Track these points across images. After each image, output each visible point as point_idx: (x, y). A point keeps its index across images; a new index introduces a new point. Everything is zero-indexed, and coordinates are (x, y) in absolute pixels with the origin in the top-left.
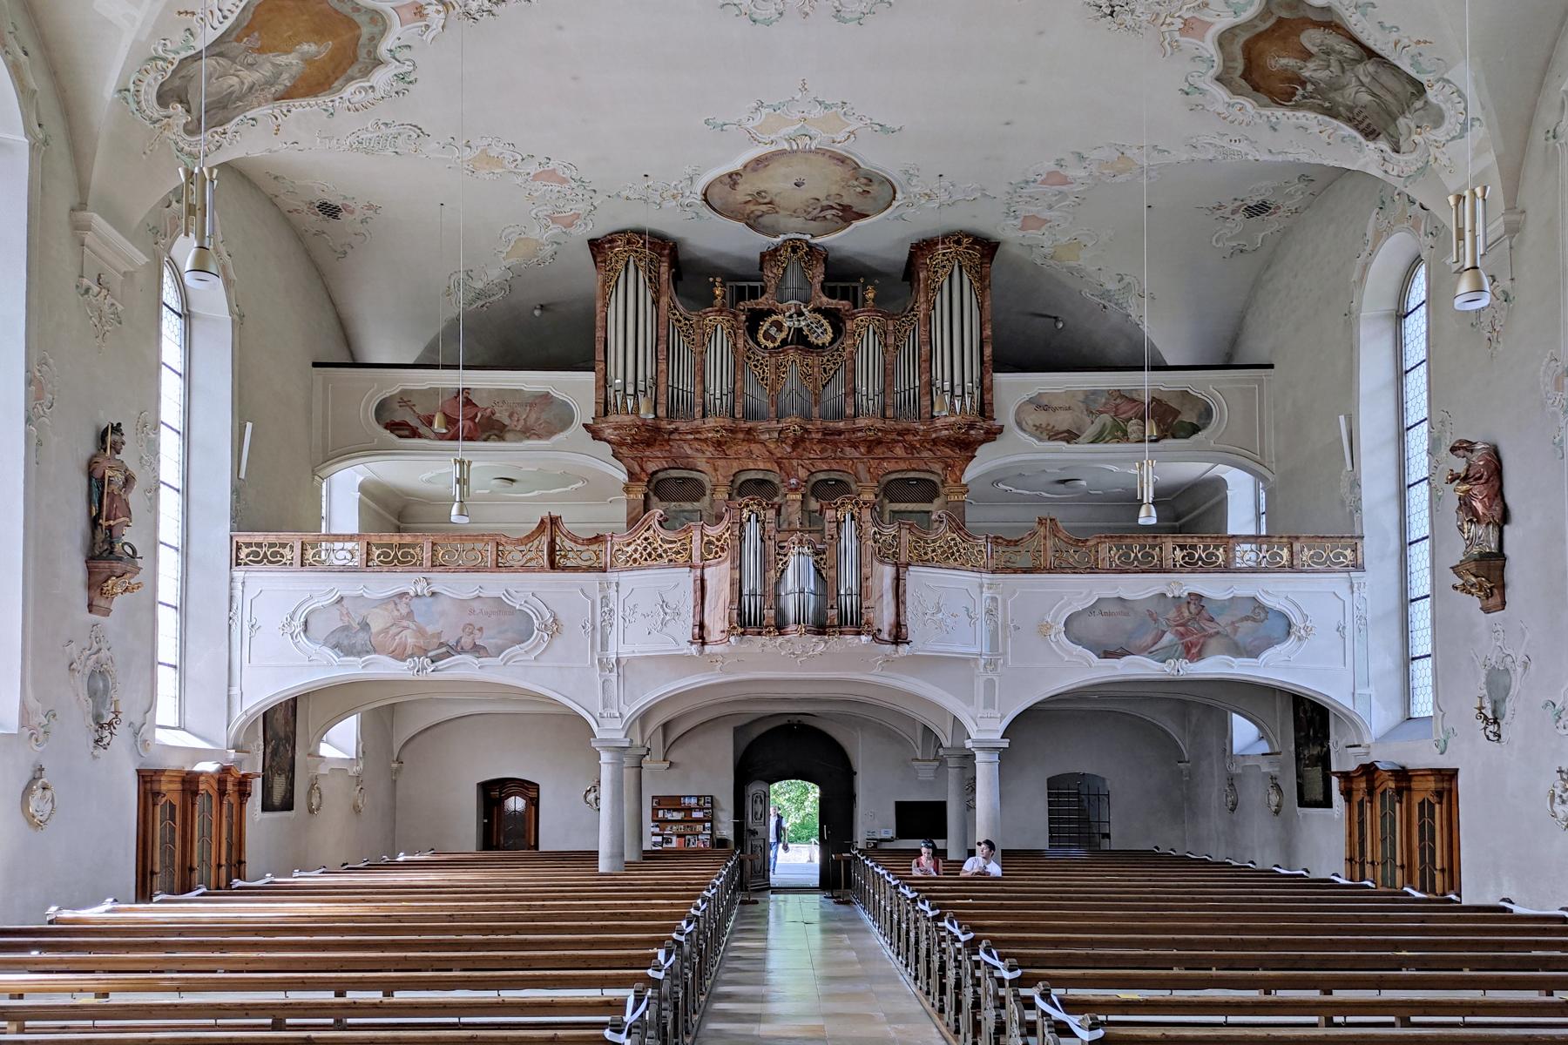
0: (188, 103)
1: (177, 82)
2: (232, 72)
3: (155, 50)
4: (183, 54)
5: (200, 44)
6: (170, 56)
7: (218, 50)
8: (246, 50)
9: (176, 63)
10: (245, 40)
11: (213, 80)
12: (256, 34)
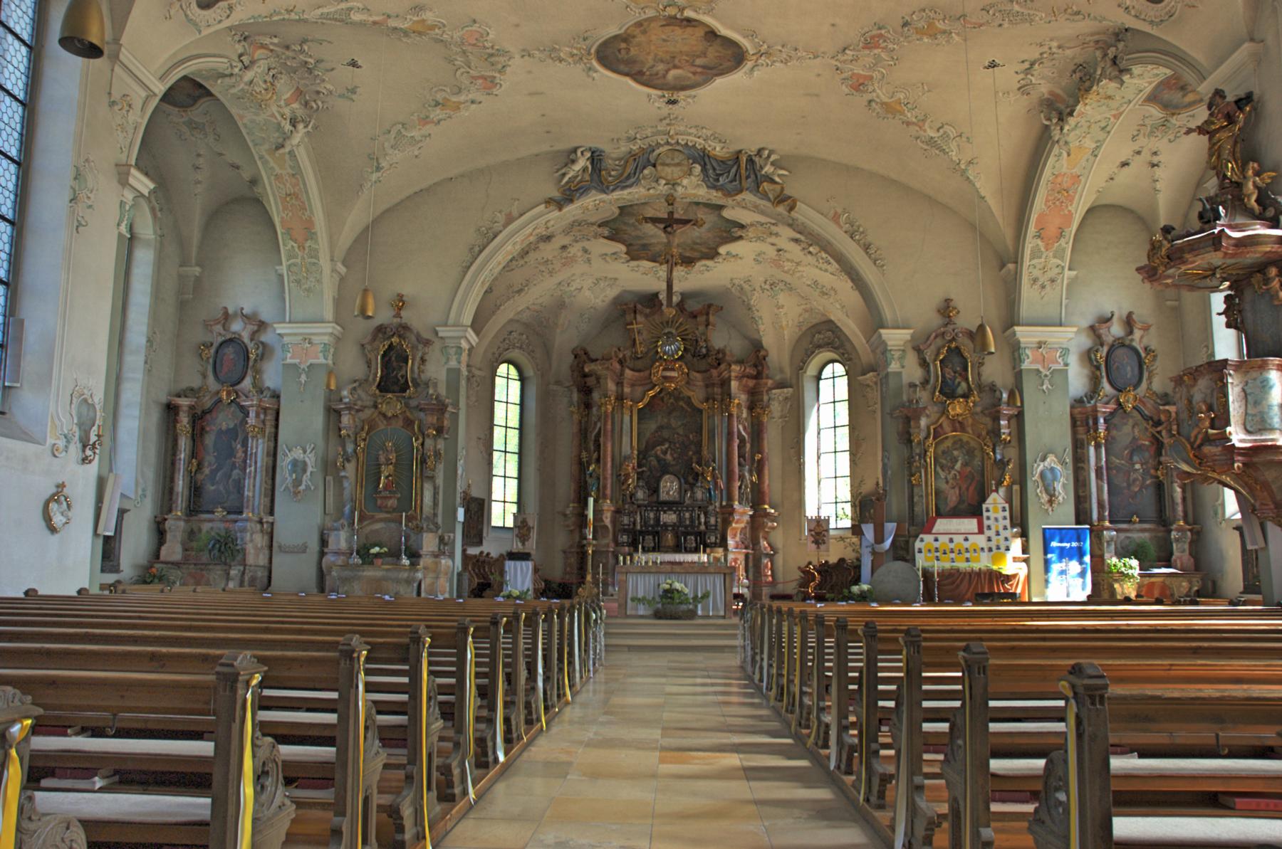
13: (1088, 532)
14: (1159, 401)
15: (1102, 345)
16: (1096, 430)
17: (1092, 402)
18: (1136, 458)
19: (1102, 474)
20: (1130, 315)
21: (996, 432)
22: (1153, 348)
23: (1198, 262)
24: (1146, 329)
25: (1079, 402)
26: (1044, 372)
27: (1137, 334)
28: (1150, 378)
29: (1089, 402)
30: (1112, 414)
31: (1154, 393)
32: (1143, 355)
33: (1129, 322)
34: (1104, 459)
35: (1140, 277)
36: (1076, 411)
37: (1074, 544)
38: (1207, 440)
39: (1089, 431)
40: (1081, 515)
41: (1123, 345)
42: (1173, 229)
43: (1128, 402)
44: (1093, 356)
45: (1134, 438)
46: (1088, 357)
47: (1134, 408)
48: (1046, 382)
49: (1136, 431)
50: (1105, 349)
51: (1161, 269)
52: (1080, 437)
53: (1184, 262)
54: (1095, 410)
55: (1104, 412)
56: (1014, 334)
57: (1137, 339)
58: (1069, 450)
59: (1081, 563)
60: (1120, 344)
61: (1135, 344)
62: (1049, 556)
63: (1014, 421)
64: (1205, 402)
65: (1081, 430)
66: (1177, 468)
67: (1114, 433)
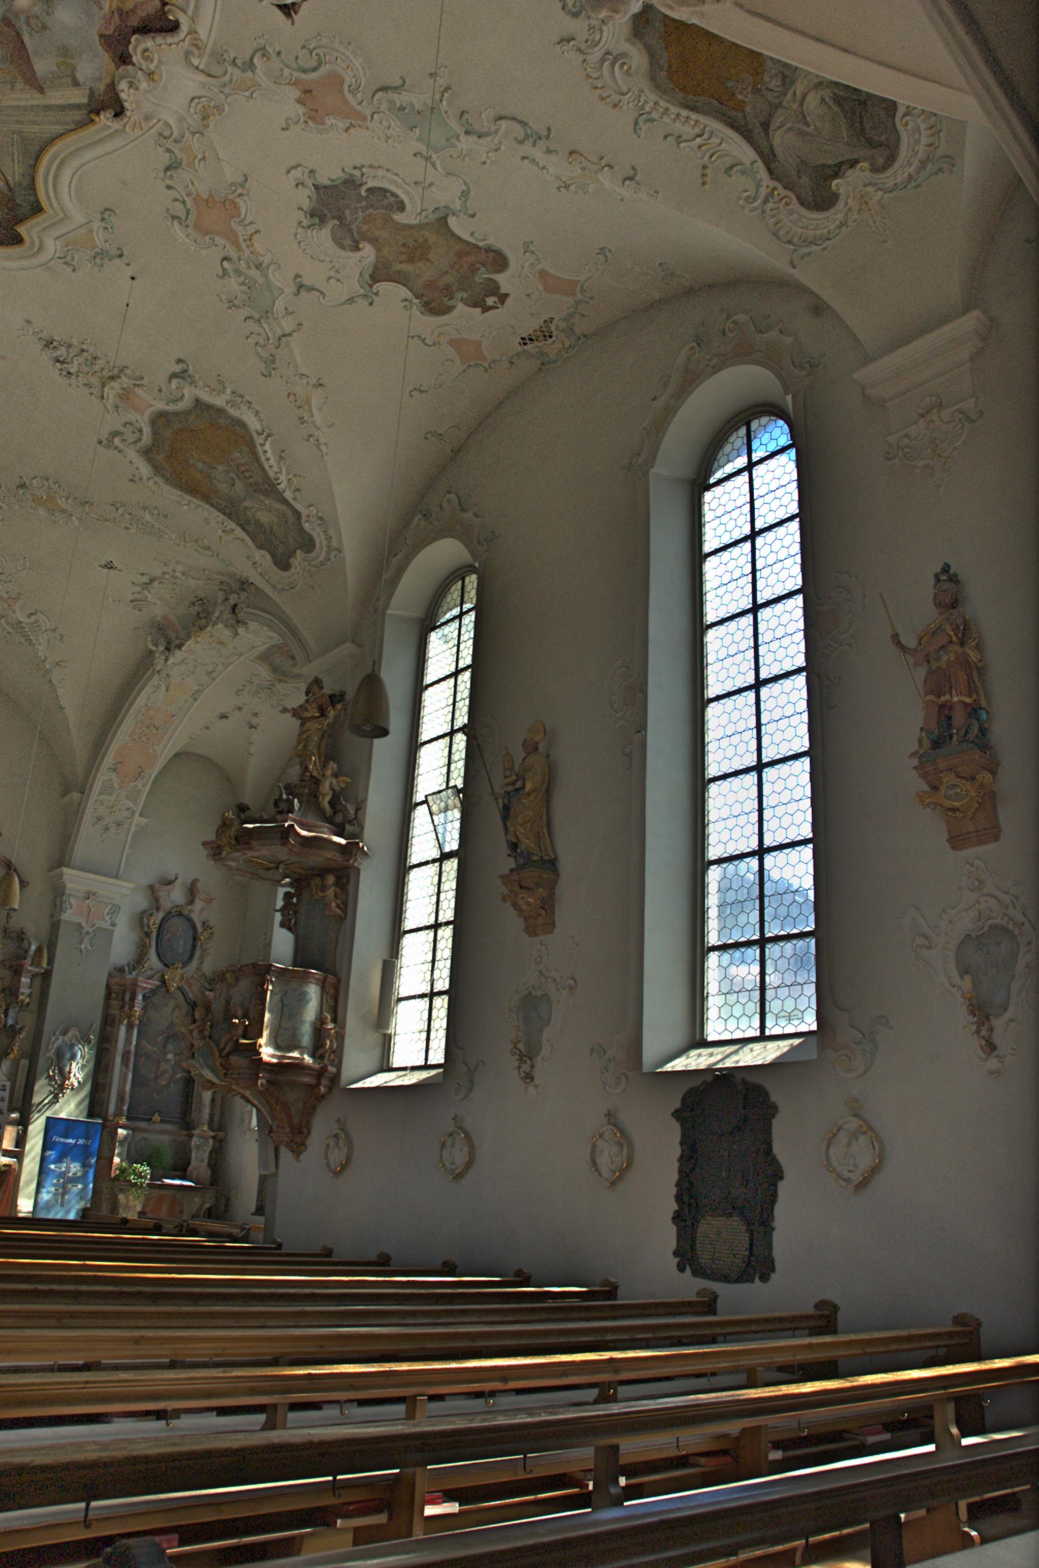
0: (841, 163)
1: (805, 180)
2: (795, 106)
3: (753, 210)
4: (763, 173)
5: (746, 153)
6: (764, 191)
7: (758, 131)
8: (756, 91)
9: (773, 184)
10: (740, 97)
11: (810, 129)
12: (730, 84)
13: (99, 1127)
14: (206, 985)
15: (158, 909)
16: (131, 1007)
17: (134, 973)
18: (170, 1047)
19: (128, 1059)
20: (194, 883)
21: (12, 991)
22: (211, 924)
23: (264, 852)
24: (209, 901)
25: (121, 970)
26: (87, 928)
27: (198, 905)
28: (202, 958)
29: (130, 973)
30: (154, 991)
31: (204, 975)
32: (200, 929)
33: (192, 891)
34: (134, 1043)
35: (204, 852)
36: (114, 981)
37: (81, 1142)
38: (238, 1048)
39: (123, 1007)
40: (95, 1105)
41: (180, 914)
42: (249, 809)
43: (173, 980)
44: (145, 920)
45: (172, 1022)
46: (141, 919)
47: (178, 988)
48: (86, 940)
49: (176, 1013)
50: (161, 915)
51: (227, 849)
52: (112, 1012)
53: (251, 849)
54: (135, 984)
55: (145, 988)
56: (61, 875)
57: (197, 912)
58: (97, 1026)
59: (85, 1166)
60: (178, 913)
61: (194, 916)
62: (49, 1153)
63: (38, 981)
64: (242, 1006)
65: (115, 1004)
66: (201, 1075)
67: (151, 1013)
